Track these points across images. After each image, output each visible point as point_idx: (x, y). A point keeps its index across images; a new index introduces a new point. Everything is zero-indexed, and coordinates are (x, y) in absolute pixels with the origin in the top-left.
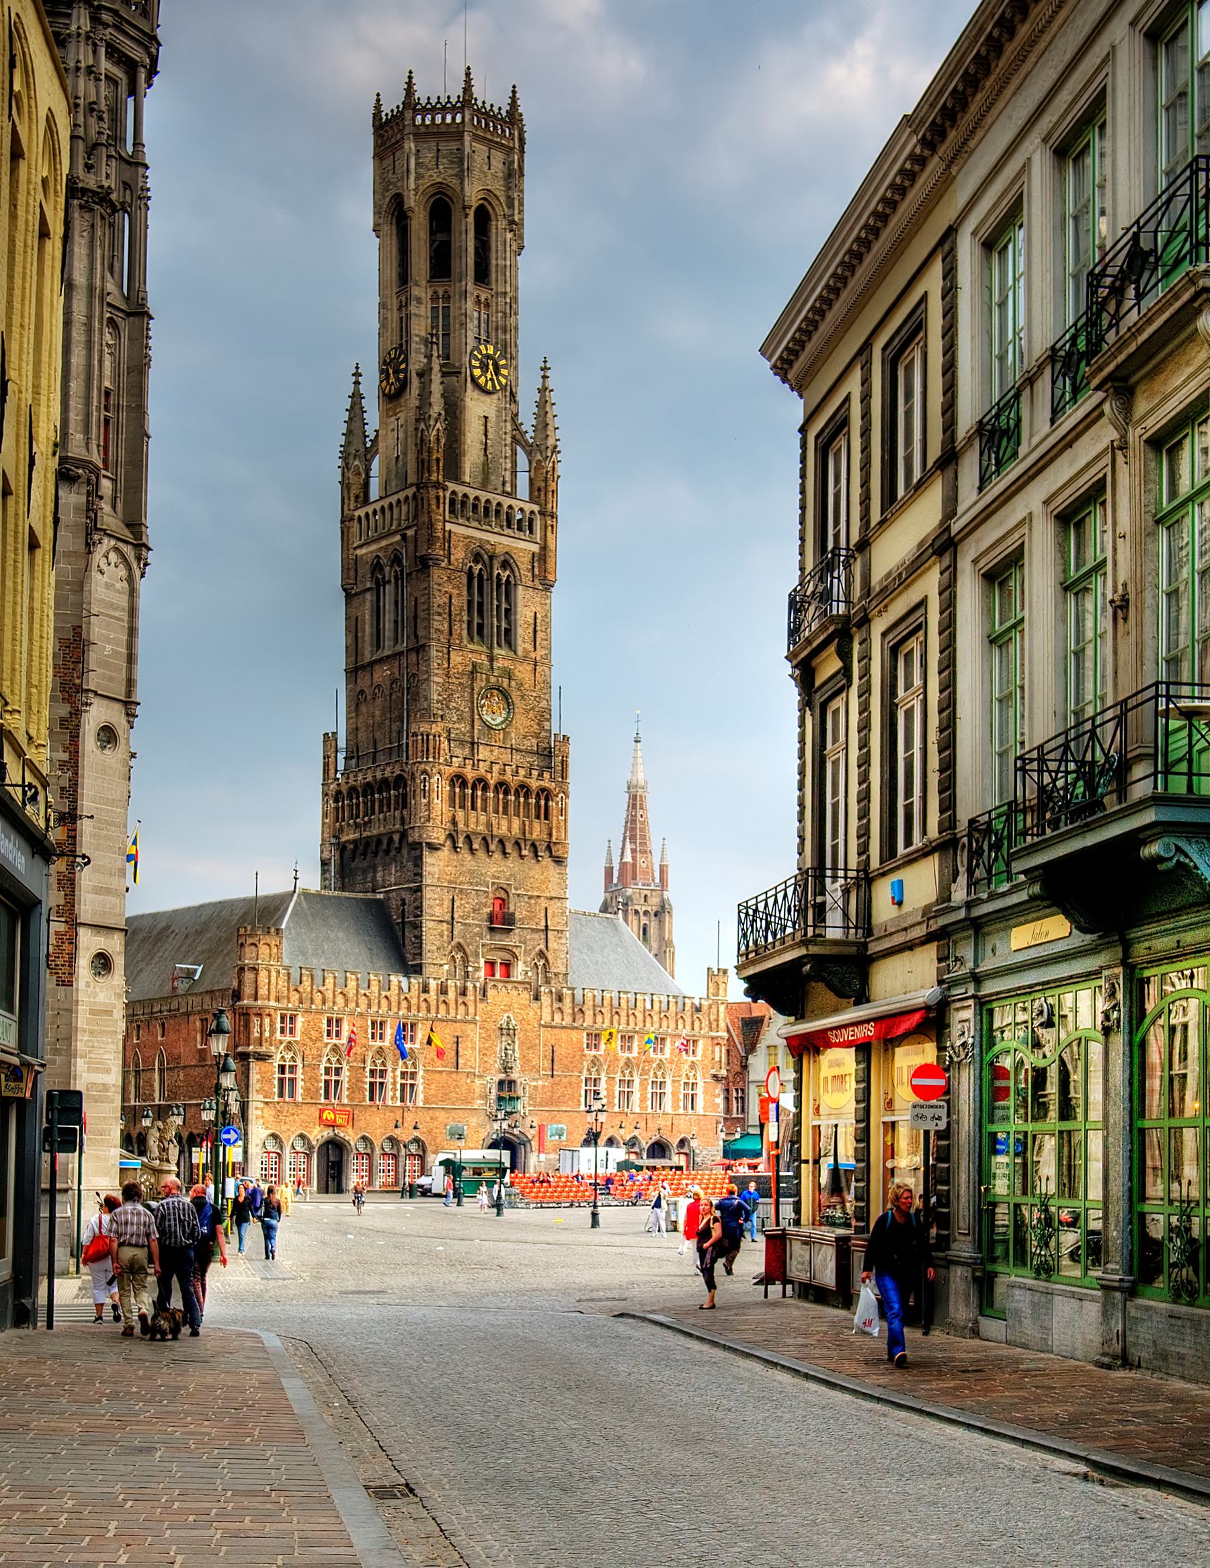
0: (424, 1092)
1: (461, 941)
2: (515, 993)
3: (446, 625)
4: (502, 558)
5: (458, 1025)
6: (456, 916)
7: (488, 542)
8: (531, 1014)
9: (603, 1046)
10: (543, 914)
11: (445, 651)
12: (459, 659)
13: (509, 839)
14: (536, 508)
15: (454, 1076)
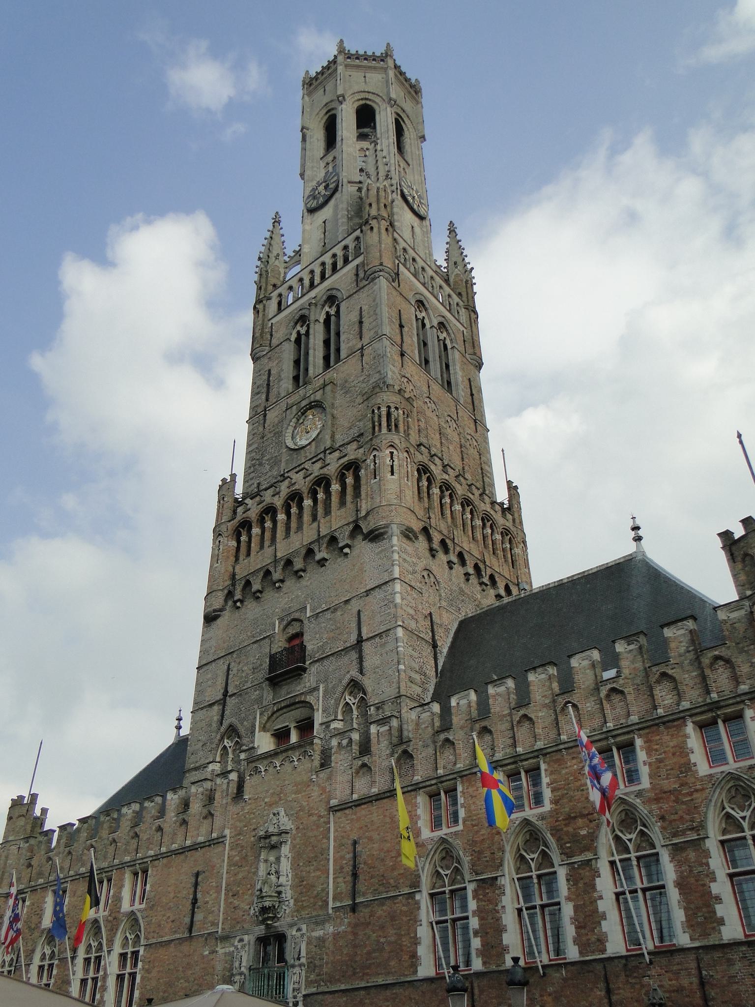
0: (143, 987)
1: (233, 719)
2: (288, 767)
3: (264, 397)
4: (325, 298)
5: (200, 852)
6: (231, 690)
7: (310, 299)
8: (315, 792)
9: (462, 813)
10: (354, 625)
11: (261, 418)
12: (276, 414)
13: (296, 552)
14: (358, 233)
15: (186, 948)
